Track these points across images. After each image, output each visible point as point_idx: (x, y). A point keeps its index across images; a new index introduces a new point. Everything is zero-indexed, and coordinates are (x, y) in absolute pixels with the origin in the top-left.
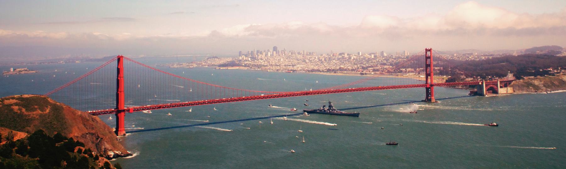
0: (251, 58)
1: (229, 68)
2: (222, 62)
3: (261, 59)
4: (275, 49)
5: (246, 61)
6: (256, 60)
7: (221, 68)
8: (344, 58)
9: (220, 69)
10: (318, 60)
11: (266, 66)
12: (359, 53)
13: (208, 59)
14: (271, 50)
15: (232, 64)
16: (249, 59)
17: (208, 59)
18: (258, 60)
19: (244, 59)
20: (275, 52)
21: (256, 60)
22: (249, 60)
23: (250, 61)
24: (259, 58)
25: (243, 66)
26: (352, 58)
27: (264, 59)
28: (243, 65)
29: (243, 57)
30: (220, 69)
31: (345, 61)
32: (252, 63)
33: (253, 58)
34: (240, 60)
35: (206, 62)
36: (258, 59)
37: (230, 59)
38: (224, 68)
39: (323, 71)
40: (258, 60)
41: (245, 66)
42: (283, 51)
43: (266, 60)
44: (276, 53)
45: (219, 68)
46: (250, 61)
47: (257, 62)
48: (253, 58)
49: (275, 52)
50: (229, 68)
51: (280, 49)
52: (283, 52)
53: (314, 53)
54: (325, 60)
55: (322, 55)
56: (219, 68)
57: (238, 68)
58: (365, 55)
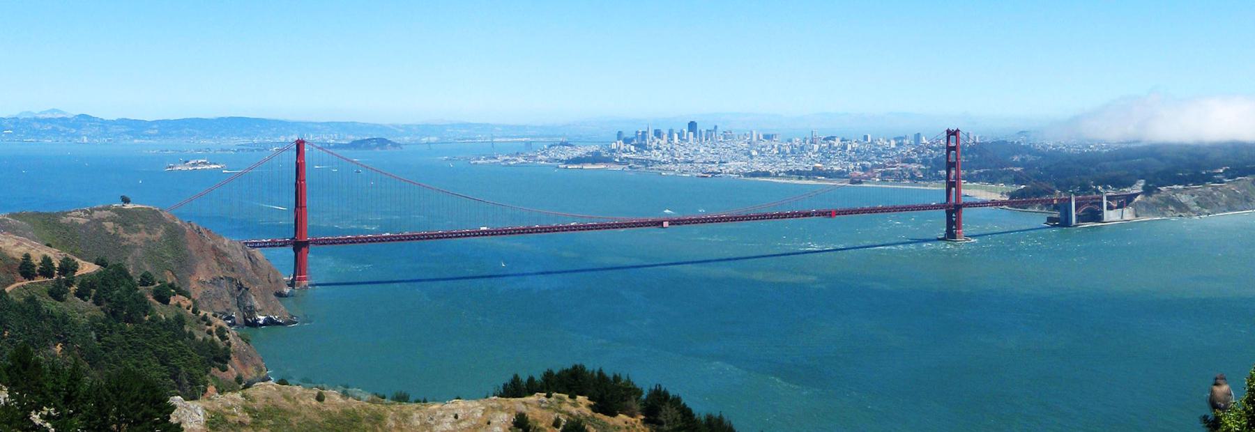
0: (635, 145)
1: (585, 167)
2: (579, 152)
3: (658, 149)
4: (692, 126)
5: (625, 152)
7: (569, 167)
9: (566, 168)
12: (866, 138)
13: (550, 147)
14: (686, 130)
15: (595, 158)
16: (633, 148)
17: (550, 147)
18: (650, 150)
19: (622, 148)
20: (691, 134)
21: (645, 151)
22: (631, 151)
23: (634, 153)
24: (652, 147)
26: (849, 148)
28: (617, 160)
29: (618, 145)
30: (566, 168)
32: (639, 156)
33: (641, 147)
34: (614, 151)
35: (544, 154)
37: (593, 148)
38: (576, 167)
39: (776, 175)
41: (621, 162)
42: (710, 131)
43: (667, 149)
44: (695, 136)
45: (565, 166)
46: (634, 153)
47: (646, 155)
48: (641, 147)
49: (691, 134)
50: (585, 167)
52: (710, 133)
53: (776, 135)
54: (792, 152)
55: (790, 141)
56: (565, 166)
57: (603, 166)
58: (879, 140)
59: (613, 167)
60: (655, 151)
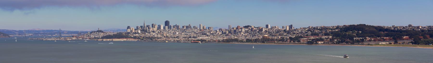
3: (154, 32)
6: (147, 32)
7: (104, 40)
8: (253, 30)
10: (221, 33)
11: (160, 38)
18: (149, 33)
20: (167, 27)
23: (140, 34)
24: (150, 31)
25: (132, 38)
27: (157, 32)
31: (256, 33)
32: (143, 35)
36: (150, 32)
40: (149, 33)
43: (158, 32)
49: (167, 27)
51: (171, 24)
57: (125, 40)
59: (131, 40)
60: (152, 33)
